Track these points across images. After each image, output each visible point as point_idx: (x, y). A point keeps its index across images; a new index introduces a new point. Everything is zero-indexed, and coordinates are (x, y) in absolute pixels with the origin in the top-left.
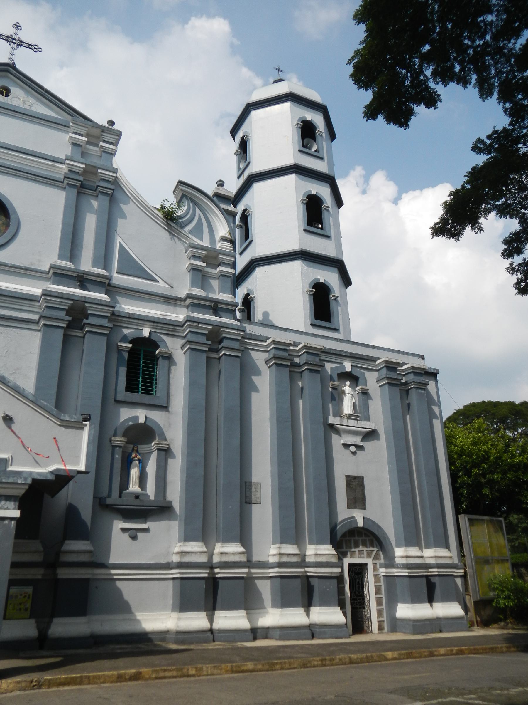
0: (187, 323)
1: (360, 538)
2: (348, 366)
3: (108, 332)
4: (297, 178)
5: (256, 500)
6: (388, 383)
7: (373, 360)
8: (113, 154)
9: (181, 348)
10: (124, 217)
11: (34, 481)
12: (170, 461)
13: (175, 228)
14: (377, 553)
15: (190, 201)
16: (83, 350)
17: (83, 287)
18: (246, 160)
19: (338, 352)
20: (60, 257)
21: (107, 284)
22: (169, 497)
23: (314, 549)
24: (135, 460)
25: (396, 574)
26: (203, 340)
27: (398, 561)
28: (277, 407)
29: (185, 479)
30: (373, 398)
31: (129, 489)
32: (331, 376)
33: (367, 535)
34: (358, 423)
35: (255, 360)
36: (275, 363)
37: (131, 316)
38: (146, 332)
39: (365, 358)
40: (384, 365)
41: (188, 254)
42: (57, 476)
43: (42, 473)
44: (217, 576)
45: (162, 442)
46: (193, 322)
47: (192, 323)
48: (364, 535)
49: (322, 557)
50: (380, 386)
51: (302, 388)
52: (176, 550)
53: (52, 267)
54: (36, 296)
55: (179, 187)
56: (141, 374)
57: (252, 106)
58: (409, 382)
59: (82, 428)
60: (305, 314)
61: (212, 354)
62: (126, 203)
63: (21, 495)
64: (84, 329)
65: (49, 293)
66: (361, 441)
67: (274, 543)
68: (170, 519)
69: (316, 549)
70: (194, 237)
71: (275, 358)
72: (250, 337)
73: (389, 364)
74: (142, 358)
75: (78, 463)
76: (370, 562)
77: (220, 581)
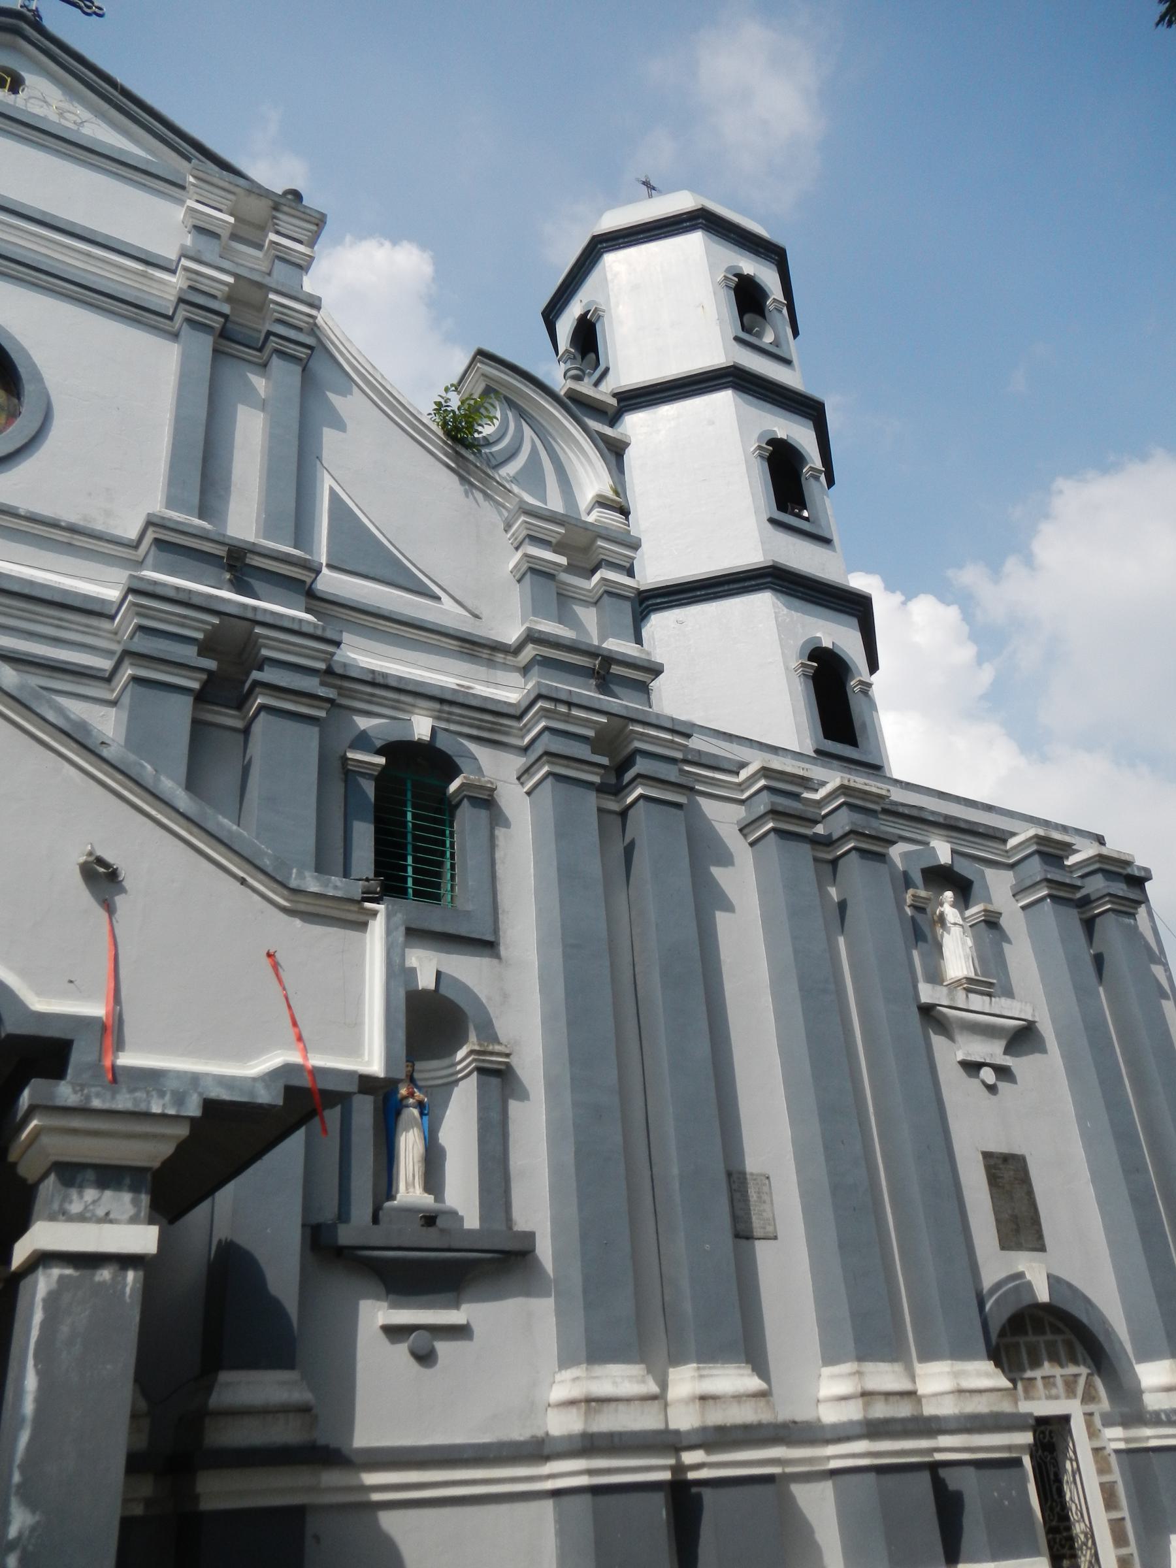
0: (539, 704)
1: (1041, 1339)
2: (943, 851)
3: (322, 714)
4: (739, 400)
5: (765, 1228)
6: (1050, 896)
7: (1000, 837)
8: (303, 266)
9: (519, 778)
10: (339, 425)
11: (211, 1106)
12: (514, 1106)
13: (477, 467)
14: (1089, 1385)
15: (506, 405)
16: (246, 771)
19: (915, 813)
20: (171, 503)
21: (307, 587)
22: (522, 1223)
23: (948, 1373)
24: (407, 1106)
25: (1153, 1443)
26: (582, 751)
27: (1153, 1402)
28: (796, 952)
29: (569, 1158)
30: (1012, 939)
31: (399, 1196)
32: (905, 874)
33: (1056, 1330)
34: (993, 1004)
35: (717, 825)
36: (773, 829)
37: (380, 680)
38: (421, 727)
39: (981, 830)
40: (1034, 848)
41: (513, 535)
42: (291, 1092)
43: (234, 1078)
44: (692, 1475)
45: (490, 1048)
46: (557, 701)
47: (553, 704)
48: (1048, 1329)
49: (977, 1398)
50: (1023, 908)
51: (842, 906)
52: (559, 1393)
53: (151, 523)
54: (103, 601)
55: (479, 365)
56: (410, 848)
57: (606, 241)
58: (1093, 897)
59: (362, 926)
60: (797, 725)
61: (608, 799)
62: (344, 392)
63: (156, 1164)
64: (251, 700)
65: (150, 588)
66: (1008, 1051)
67: (830, 1358)
68: (528, 1294)
69: (956, 1375)
70: (528, 493)
71: (774, 813)
72: (696, 759)
73: (1045, 845)
74: (409, 804)
75: (355, 1048)
76: (1073, 1408)
77: (708, 1494)
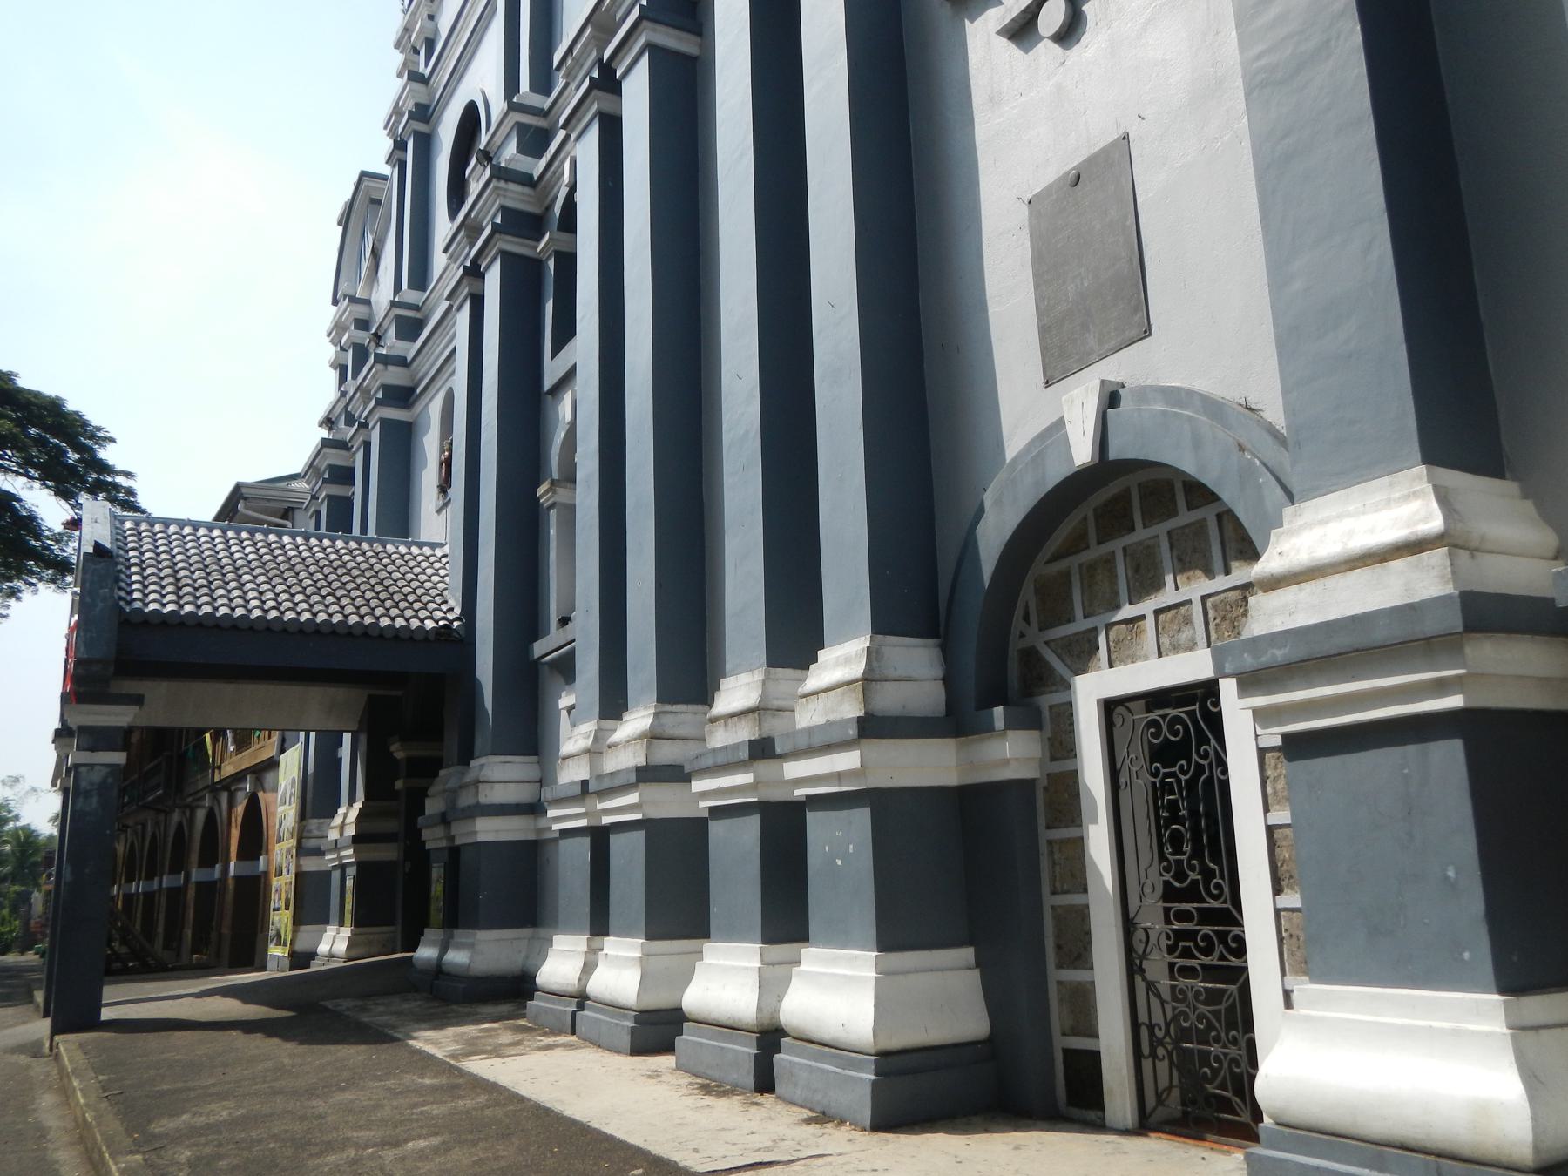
1: (1161, 529)
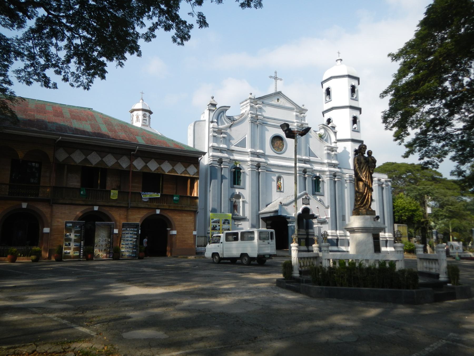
17: (305, 163)
18: (330, 99)
38: (318, 175)
68: (326, 224)
